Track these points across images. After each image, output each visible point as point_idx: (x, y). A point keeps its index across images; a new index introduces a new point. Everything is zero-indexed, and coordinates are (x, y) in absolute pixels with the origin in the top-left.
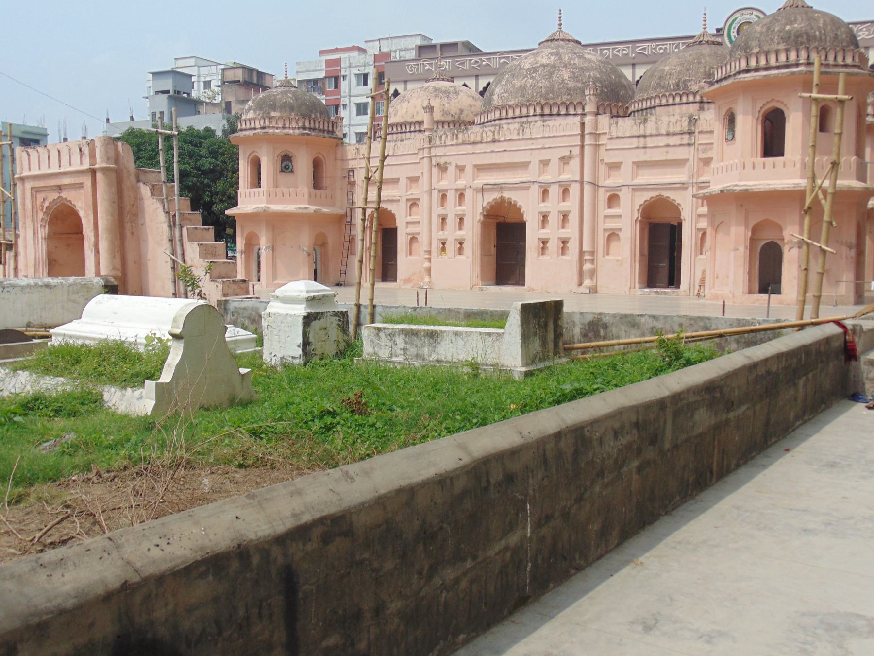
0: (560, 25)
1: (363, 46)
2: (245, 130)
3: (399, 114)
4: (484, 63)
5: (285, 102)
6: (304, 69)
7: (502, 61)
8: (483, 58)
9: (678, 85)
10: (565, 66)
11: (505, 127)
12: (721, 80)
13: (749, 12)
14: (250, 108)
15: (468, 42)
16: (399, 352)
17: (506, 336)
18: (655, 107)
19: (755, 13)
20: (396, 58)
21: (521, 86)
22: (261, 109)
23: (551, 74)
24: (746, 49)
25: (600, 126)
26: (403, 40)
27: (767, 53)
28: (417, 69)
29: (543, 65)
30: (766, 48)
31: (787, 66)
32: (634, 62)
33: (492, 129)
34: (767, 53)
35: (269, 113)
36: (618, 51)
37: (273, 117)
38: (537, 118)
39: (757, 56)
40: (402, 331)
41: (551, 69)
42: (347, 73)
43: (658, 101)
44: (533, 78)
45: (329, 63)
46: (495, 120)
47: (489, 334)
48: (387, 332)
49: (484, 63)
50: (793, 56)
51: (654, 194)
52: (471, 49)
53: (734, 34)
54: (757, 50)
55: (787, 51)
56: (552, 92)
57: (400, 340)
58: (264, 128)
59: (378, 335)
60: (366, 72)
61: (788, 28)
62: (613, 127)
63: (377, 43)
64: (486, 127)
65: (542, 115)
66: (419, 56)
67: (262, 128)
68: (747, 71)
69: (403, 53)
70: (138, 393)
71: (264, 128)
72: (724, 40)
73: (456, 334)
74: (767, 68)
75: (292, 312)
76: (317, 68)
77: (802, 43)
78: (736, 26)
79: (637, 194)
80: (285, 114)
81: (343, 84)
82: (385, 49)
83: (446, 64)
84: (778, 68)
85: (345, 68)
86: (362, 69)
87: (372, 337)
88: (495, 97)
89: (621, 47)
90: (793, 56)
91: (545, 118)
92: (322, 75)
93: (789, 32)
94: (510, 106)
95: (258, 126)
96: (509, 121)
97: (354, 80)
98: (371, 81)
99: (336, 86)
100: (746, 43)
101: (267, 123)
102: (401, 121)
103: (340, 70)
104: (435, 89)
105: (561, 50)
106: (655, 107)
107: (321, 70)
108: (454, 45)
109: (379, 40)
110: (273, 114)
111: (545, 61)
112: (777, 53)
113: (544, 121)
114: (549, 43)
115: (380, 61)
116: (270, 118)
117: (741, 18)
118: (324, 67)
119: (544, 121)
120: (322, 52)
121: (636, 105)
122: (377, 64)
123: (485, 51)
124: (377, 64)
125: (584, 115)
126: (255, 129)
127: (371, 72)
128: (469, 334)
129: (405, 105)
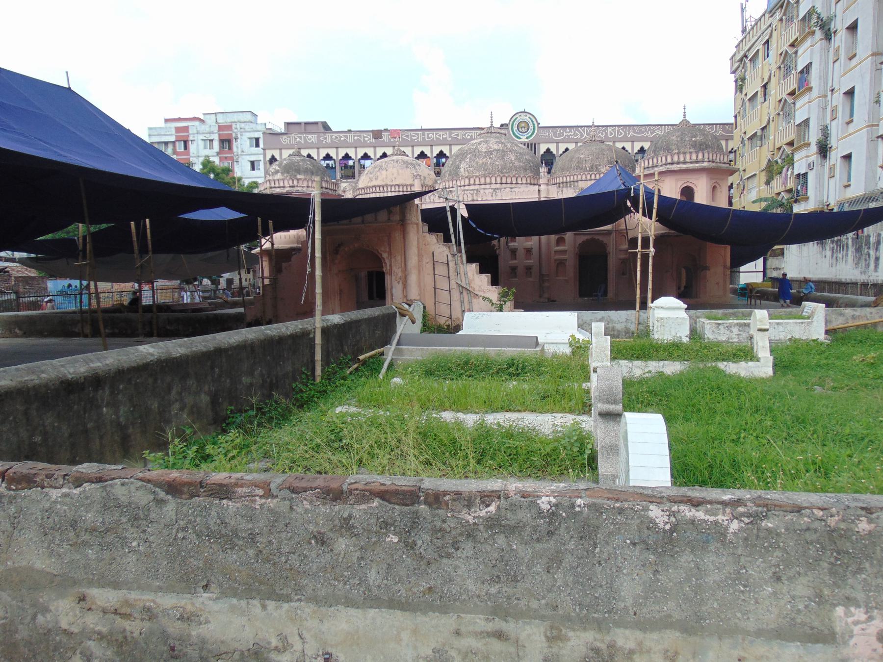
0: (492, 122)
1: (202, 117)
2: (275, 187)
3: (380, 178)
4: (342, 139)
5: (307, 168)
6: (156, 133)
7: (356, 138)
8: (341, 135)
9: (592, 168)
10: (510, 151)
11: (482, 191)
12: (648, 168)
13: (524, 114)
14: (277, 172)
15: (325, 123)
16: (734, 336)
17: (815, 323)
18: (577, 181)
19: (528, 115)
20: (236, 129)
21: (483, 163)
22: (288, 173)
23: (503, 156)
24: (668, 150)
25: (550, 193)
26: (236, 114)
27: (685, 153)
28: (290, 141)
29: (495, 150)
30: (682, 150)
31: (697, 162)
32: (451, 143)
33: (472, 192)
34: (685, 153)
35: (296, 176)
36: (440, 136)
37: (301, 179)
38: (498, 186)
39: (678, 154)
40: (737, 324)
41: (503, 153)
42: (195, 139)
43: (579, 177)
44: (490, 158)
45: (178, 130)
46: (464, 186)
47: (802, 323)
48: (725, 325)
49: (342, 139)
50: (700, 156)
51: (589, 237)
52: (326, 127)
53: (515, 128)
54: (677, 151)
55: (697, 153)
56: (506, 168)
57: (735, 330)
58: (293, 187)
59: (718, 327)
60: (211, 138)
61: (694, 139)
62: (560, 193)
63: (214, 116)
64: (467, 190)
65: (501, 183)
66: (288, 130)
67: (290, 187)
68: (672, 164)
69: (243, 125)
70: (750, 364)
71: (293, 187)
72: (509, 132)
73: (778, 324)
74: (685, 163)
75: (672, 316)
76: (168, 133)
77: (703, 150)
78: (516, 123)
79: (577, 237)
80: (308, 177)
81: (192, 148)
82: (221, 120)
83: (312, 138)
84: (691, 163)
85: (194, 134)
86: (208, 135)
87: (713, 329)
88: (462, 170)
89: (441, 133)
90: (700, 156)
91: (513, 186)
92: (173, 139)
93: (695, 142)
94: (477, 177)
95: (286, 184)
96: (483, 187)
97: (201, 144)
98: (216, 144)
99: (186, 148)
100: (668, 147)
101: (295, 183)
102: (383, 184)
103: (188, 136)
104: (405, 162)
105: (503, 141)
106: (577, 181)
107: (171, 135)
108: (316, 123)
109: (216, 114)
110: (299, 177)
111: (495, 147)
112: (691, 153)
113: (511, 188)
114: (489, 135)
115: (223, 131)
116: (298, 180)
117: (520, 118)
118: (173, 132)
119: (511, 188)
120: (167, 121)
121: (561, 179)
122: (221, 133)
123: (334, 130)
124: (221, 133)
125: (540, 185)
126: (284, 187)
127: (216, 137)
128: (787, 324)
129: (384, 172)
